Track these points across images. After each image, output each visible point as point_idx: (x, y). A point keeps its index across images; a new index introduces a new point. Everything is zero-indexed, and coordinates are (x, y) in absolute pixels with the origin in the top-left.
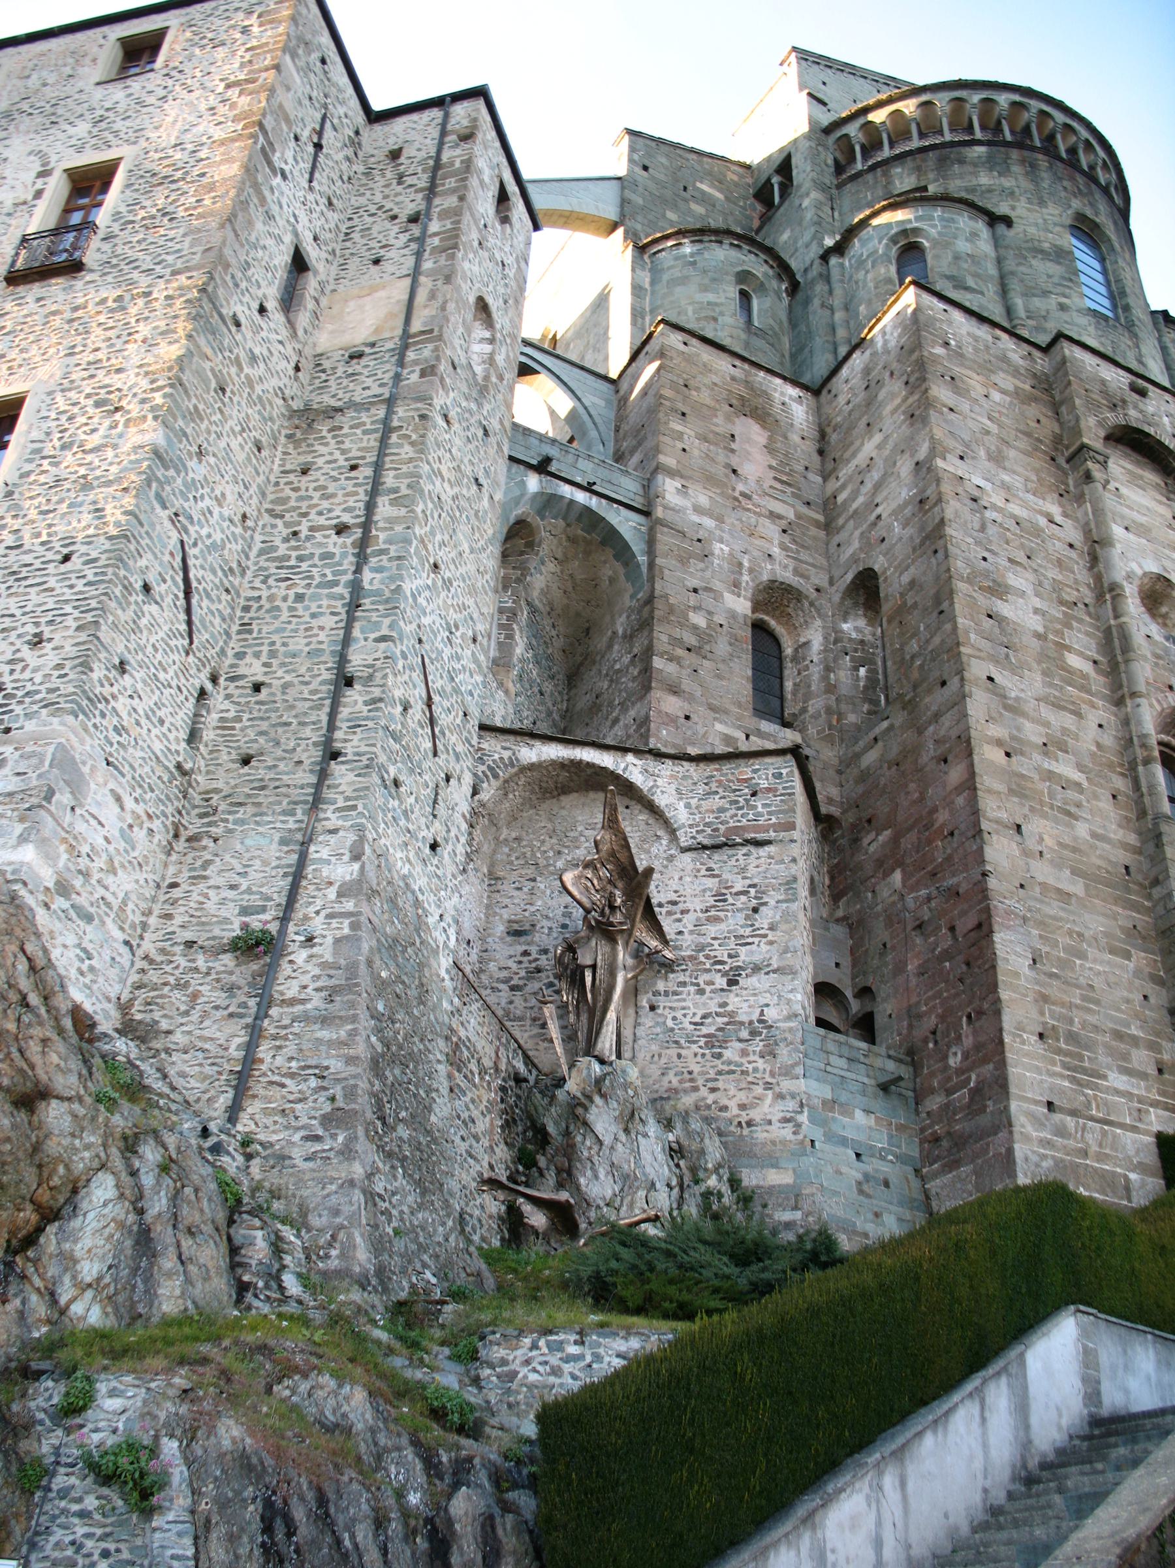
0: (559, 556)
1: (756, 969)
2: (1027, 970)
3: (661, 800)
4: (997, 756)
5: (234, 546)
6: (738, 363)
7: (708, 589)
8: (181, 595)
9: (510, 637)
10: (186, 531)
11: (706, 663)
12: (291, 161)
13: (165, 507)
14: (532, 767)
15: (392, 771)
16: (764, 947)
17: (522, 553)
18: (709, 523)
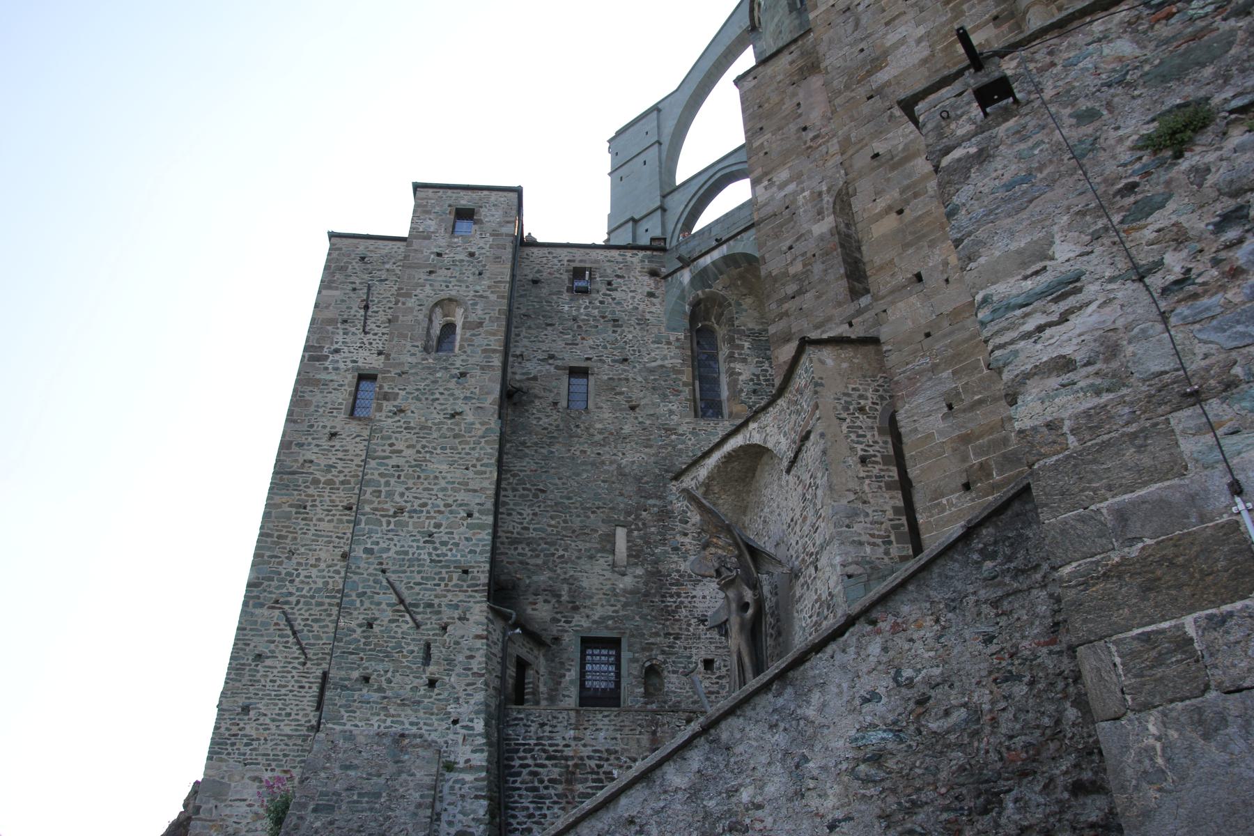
0: (745, 291)
1: (822, 548)
2: (942, 425)
3: (770, 445)
4: (892, 221)
5: (337, 577)
6: (793, 48)
7: (798, 239)
8: (291, 639)
9: (732, 373)
10: (287, 603)
11: (808, 295)
12: (340, 338)
13: (262, 605)
14: (711, 478)
15: (355, 674)
16: (823, 525)
17: (722, 314)
18: (792, 187)
